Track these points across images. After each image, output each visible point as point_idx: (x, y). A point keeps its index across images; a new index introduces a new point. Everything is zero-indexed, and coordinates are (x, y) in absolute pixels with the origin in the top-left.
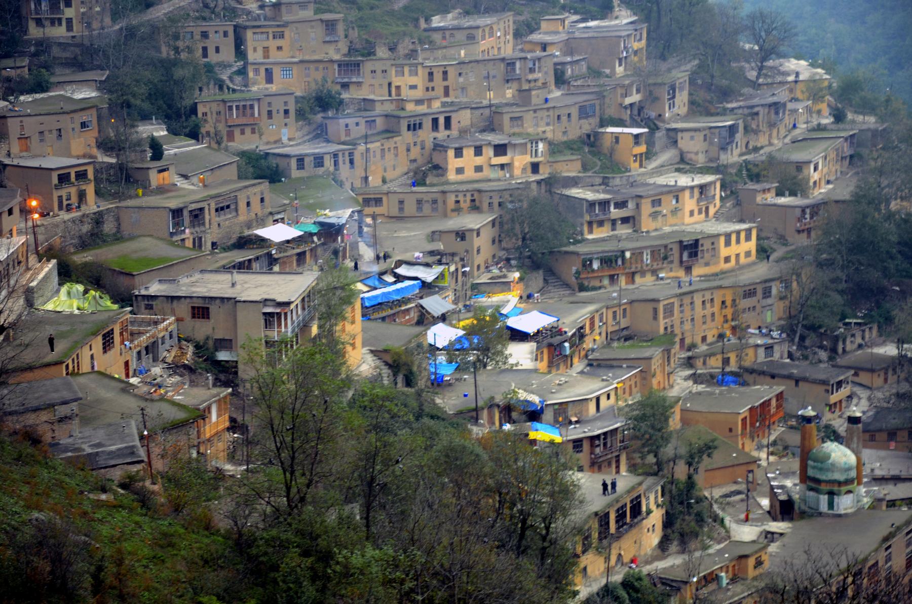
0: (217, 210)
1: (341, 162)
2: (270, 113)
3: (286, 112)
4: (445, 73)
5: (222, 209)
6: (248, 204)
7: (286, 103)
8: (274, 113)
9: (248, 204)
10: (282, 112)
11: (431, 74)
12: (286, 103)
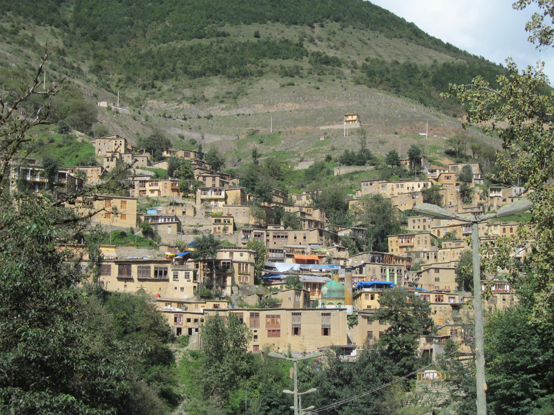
0: (274, 237)
1: (430, 257)
2: (419, 241)
3: (426, 241)
4: (511, 229)
5: (279, 237)
6: (295, 238)
7: (426, 237)
8: (421, 242)
9: (295, 238)
10: (424, 241)
11: (504, 229)
12: (426, 237)
